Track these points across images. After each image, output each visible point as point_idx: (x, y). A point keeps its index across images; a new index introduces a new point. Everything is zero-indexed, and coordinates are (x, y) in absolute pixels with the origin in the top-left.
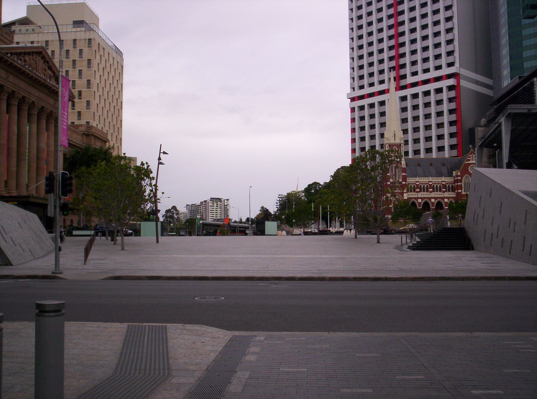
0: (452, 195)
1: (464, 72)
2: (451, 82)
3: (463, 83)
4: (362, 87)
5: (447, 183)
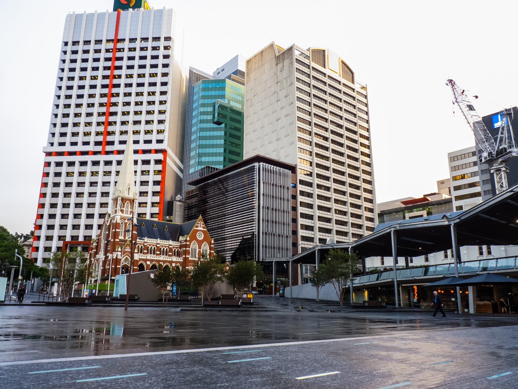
0: (181, 260)
1: (170, 152)
2: (160, 156)
3: (168, 160)
4: (62, 144)
5: (174, 247)
